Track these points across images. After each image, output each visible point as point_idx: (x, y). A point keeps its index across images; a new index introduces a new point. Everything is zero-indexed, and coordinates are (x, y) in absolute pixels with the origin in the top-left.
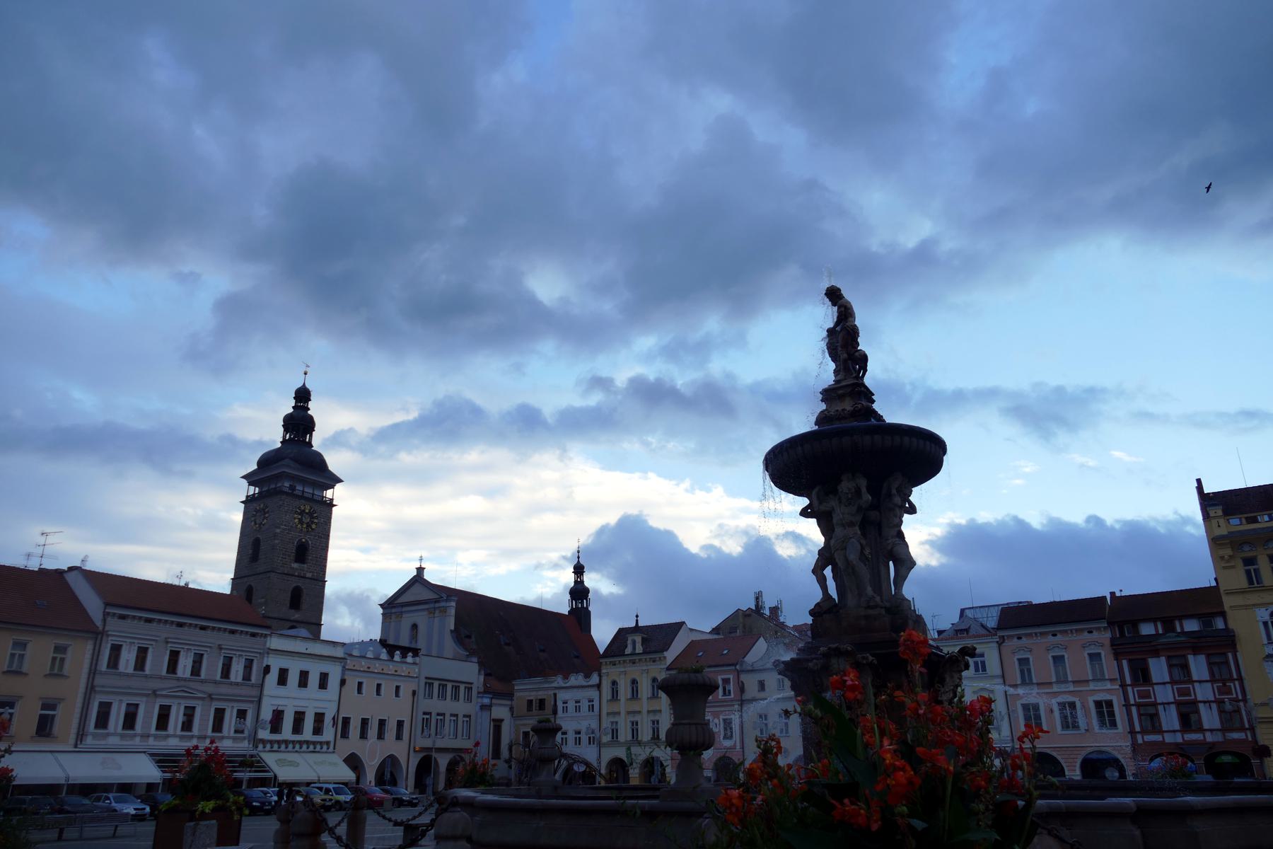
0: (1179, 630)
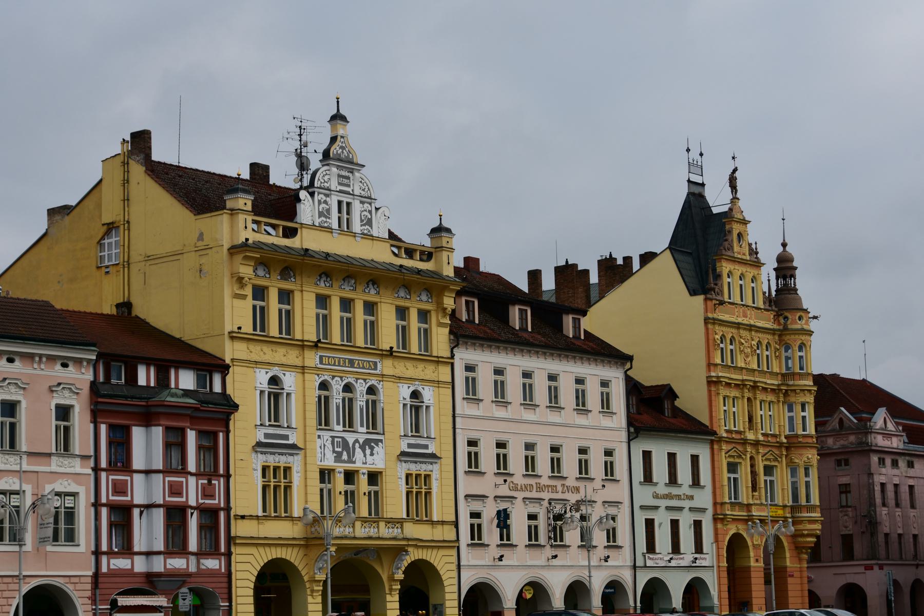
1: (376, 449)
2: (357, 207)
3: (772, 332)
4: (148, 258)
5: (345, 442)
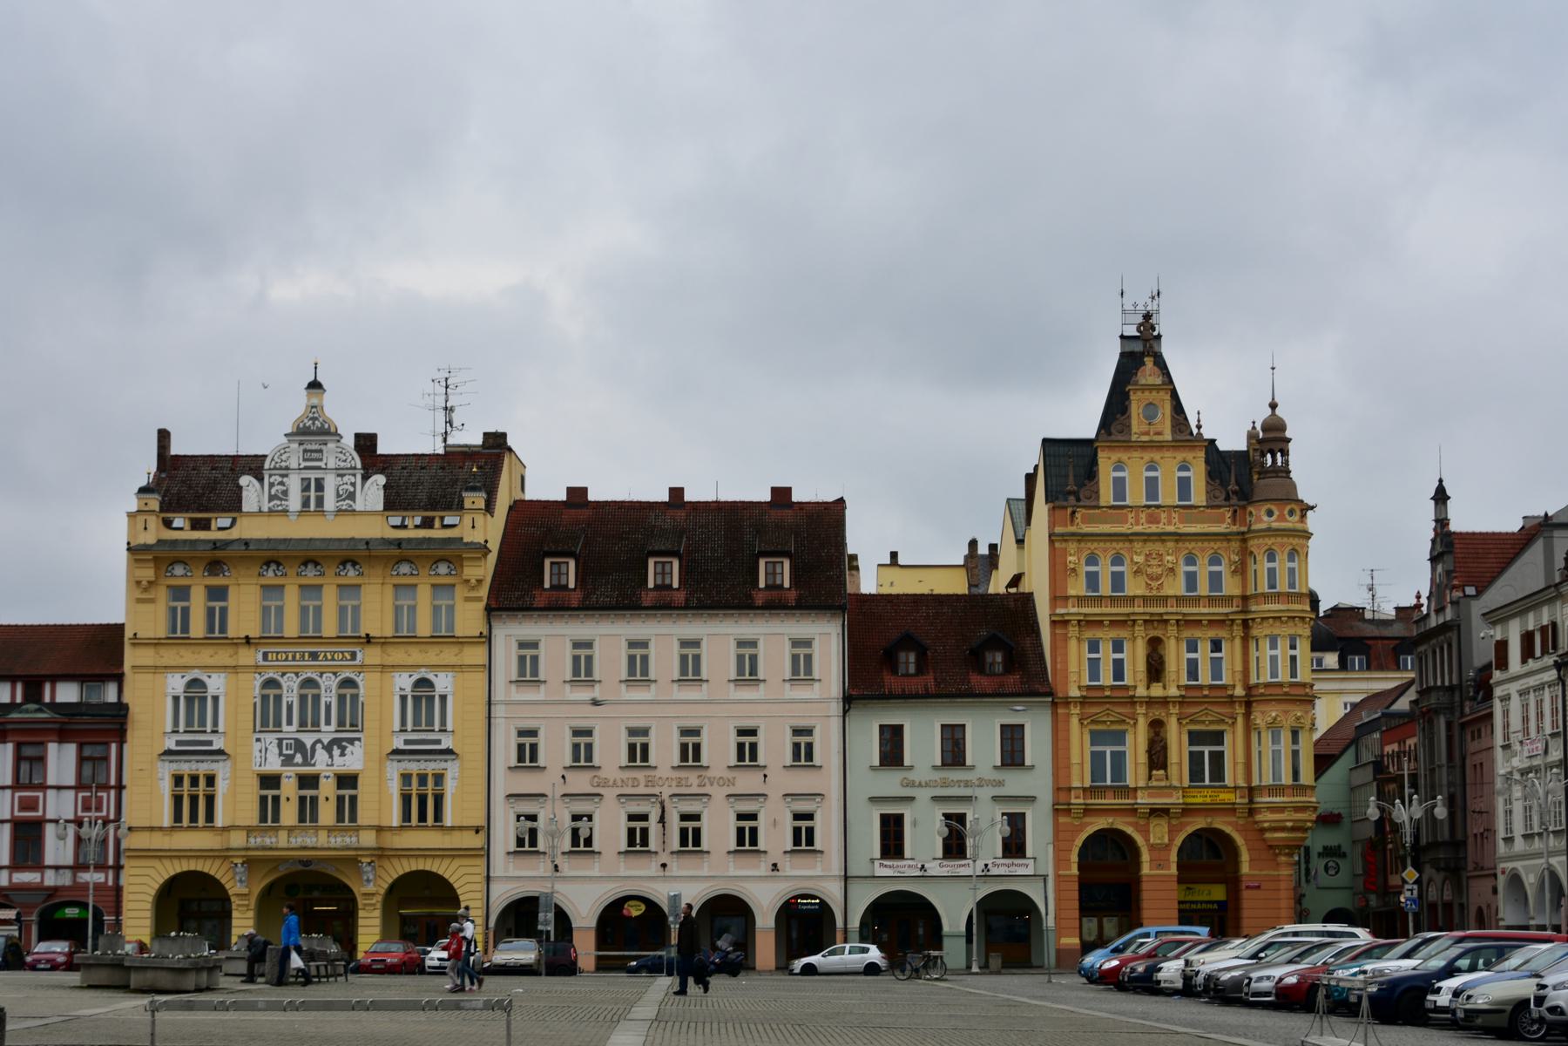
0: (47, 699)
1: (350, 748)
2: (331, 482)
3: (1225, 536)
5: (300, 746)
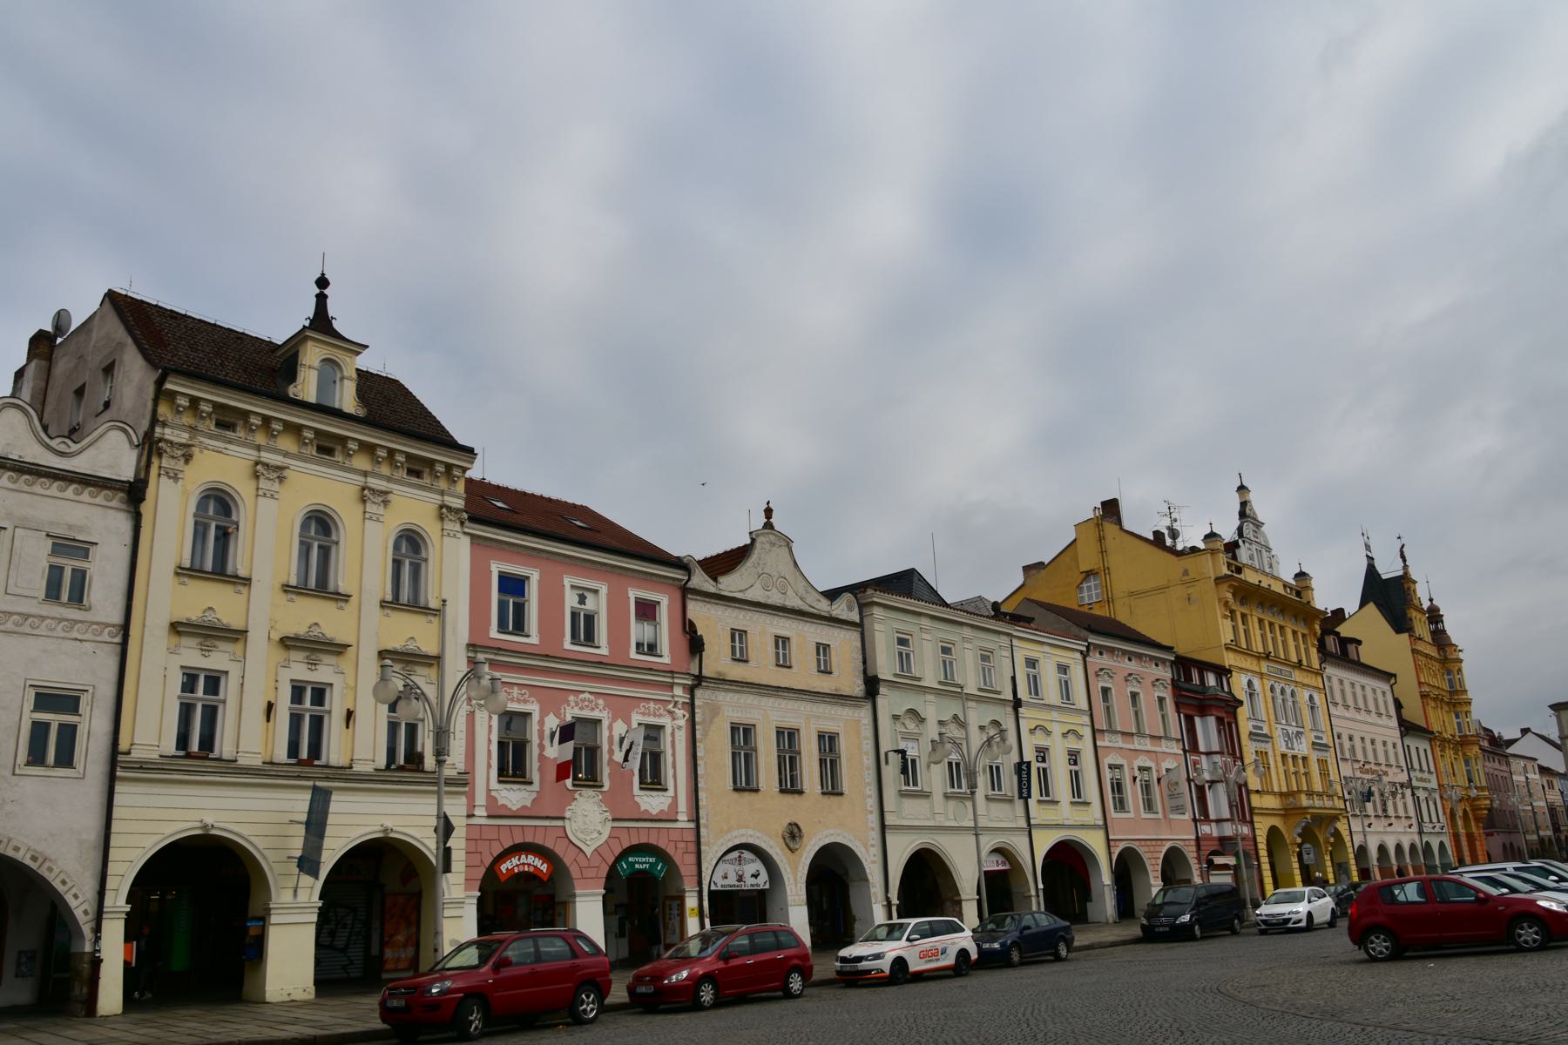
2: (1265, 554)
4: (1132, 594)
